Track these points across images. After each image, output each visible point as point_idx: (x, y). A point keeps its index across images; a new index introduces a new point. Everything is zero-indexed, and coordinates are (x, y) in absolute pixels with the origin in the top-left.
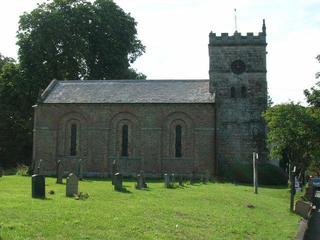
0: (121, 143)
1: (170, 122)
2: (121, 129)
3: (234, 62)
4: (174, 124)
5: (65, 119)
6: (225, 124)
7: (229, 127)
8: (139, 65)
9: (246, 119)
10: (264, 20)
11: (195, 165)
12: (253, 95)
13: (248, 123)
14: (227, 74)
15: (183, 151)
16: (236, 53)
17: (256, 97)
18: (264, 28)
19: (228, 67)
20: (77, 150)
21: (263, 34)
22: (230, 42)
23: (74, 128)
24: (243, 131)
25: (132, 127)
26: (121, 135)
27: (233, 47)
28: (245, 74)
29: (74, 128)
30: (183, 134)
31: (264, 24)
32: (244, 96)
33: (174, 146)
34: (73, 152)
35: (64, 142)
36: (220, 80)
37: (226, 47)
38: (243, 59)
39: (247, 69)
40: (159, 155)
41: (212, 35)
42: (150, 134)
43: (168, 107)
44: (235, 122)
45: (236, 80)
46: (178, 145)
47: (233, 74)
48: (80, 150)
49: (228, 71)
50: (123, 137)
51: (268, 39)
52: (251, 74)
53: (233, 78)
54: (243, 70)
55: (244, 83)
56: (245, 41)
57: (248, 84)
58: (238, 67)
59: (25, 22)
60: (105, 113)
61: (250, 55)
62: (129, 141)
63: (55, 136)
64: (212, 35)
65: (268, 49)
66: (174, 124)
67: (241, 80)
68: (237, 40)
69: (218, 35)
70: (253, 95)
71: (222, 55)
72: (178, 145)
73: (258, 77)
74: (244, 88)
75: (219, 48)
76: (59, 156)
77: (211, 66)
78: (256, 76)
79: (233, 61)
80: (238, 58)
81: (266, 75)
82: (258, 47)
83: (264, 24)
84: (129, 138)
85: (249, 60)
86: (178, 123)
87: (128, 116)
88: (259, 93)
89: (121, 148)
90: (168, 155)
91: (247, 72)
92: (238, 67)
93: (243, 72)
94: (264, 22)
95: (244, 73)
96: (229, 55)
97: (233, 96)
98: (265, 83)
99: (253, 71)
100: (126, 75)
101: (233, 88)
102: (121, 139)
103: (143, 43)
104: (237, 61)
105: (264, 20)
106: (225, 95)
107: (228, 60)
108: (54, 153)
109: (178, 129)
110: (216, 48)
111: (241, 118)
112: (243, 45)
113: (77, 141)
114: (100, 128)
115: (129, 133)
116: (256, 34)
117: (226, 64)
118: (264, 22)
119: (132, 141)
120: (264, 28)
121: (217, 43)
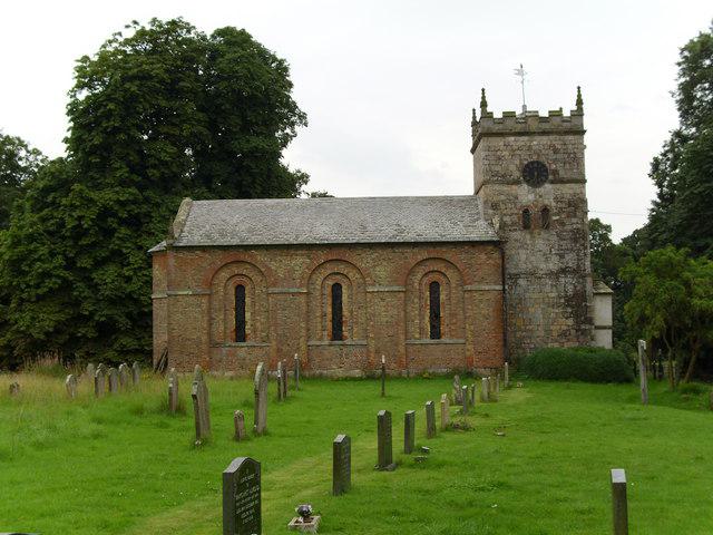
0: (330, 316)
1: (419, 276)
2: (328, 291)
3: (527, 166)
5: (224, 274)
6: (517, 276)
7: (522, 282)
8: (291, 158)
9: (551, 266)
10: (579, 88)
11: (468, 353)
12: (563, 224)
13: (555, 275)
16: (530, 148)
17: (569, 228)
18: (579, 102)
19: (517, 174)
21: (578, 113)
22: (519, 128)
23: (240, 289)
24: (548, 288)
25: (350, 286)
26: (330, 302)
27: (526, 138)
29: (240, 289)
30: (443, 297)
31: (579, 96)
32: (546, 226)
33: (427, 319)
34: (240, 334)
36: (503, 197)
37: (513, 138)
38: (543, 159)
39: (551, 177)
40: (402, 337)
43: (416, 250)
44: (532, 275)
45: (531, 197)
47: (525, 186)
49: (517, 182)
50: (333, 304)
51: (587, 123)
52: (558, 186)
53: (526, 195)
54: (544, 178)
55: (546, 202)
56: (546, 126)
57: (554, 204)
58: (535, 173)
59: (88, 73)
60: (299, 262)
61: (556, 151)
62: (345, 312)
63: (205, 307)
65: (587, 139)
66: (426, 280)
67: (540, 196)
70: (563, 224)
71: (506, 153)
73: (571, 191)
74: (545, 210)
75: (498, 139)
76: (214, 345)
78: (567, 190)
79: (526, 162)
80: (535, 158)
81: (584, 187)
82: (571, 137)
83: (579, 96)
85: (555, 161)
86: (434, 277)
87: (342, 268)
88: (574, 220)
89: (329, 325)
90: (417, 336)
91: (552, 182)
93: (544, 182)
95: (546, 185)
96: (518, 152)
97: (526, 227)
98: (584, 202)
99: (562, 181)
100: (285, 185)
101: (526, 211)
103: (302, 107)
104: (532, 163)
106: (513, 224)
107: (517, 162)
108: (204, 338)
109: (434, 287)
111: (543, 266)
112: (544, 133)
113: (248, 315)
114: (291, 290)
115: (345, 298)
117: (513, 168)
119: (351, 312)
120: (579, 102)
121: (488, 130)
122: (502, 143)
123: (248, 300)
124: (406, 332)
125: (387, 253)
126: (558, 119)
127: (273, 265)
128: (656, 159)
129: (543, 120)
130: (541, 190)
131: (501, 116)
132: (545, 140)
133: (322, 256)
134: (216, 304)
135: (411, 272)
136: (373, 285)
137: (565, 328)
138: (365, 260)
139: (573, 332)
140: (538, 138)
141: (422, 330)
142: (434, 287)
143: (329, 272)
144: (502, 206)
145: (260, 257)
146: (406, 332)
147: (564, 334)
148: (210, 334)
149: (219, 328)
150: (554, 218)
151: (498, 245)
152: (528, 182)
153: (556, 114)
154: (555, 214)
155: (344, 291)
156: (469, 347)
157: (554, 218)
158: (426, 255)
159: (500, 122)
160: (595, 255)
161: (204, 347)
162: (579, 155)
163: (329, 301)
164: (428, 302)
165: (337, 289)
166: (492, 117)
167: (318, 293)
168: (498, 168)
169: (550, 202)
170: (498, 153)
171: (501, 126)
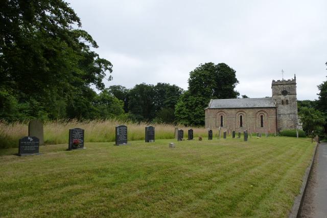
8: (237, 88)
13: (289, 114)
18: (295, 77)
19: (280, 93)
23: (222, 117)
28: (287, 96)
29: (222, 117)
30: (264, 119)
32: (287, 104)
41: (273, 81)
46: (262, 123)
49: (280, 95)
53: (282, 97)
56: (287, 83)
58: (284, 93)
59: (193, 75)
60: (233, 111)
61: (289, 88)
64: (273, 81)
65: (297, 85)
66: (261, 115)
69: (276, 81)
72: (262, 123)
74: (287, 101)
77: (273, 93)
78: (292, 96)
100: (234, 95)
103: (238, 80)
112: (287, 84)
120: (295, 77)
121: (275, 84)
132: (287, 86)
133: (238, 110)
135: (257, 113)
138: (247, 111)
141: (259, 125)
142: (262, 116)
145: (226, 111)
147: (291, 127)
151: (275, 108)
159: (277, 82)
165: (241, 117)
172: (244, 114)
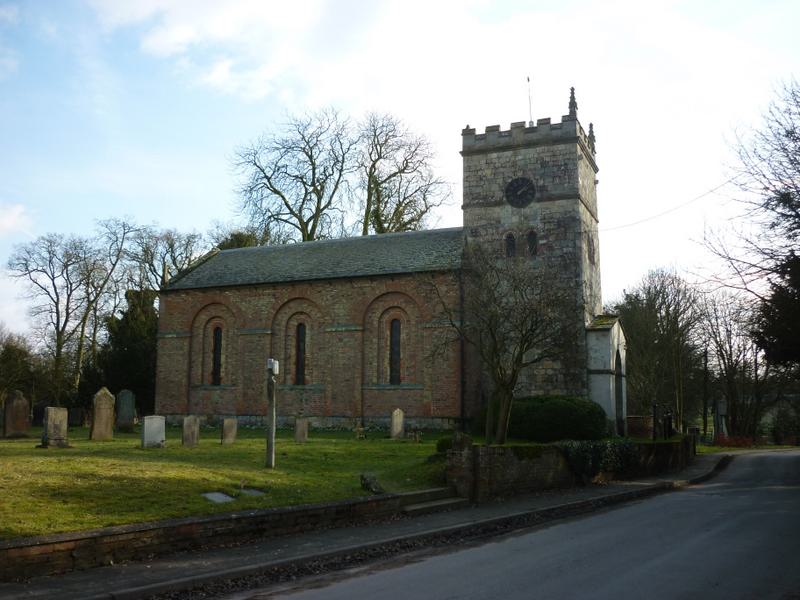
0: (293, 359)
1: (378, 314)
2: (292, 332)
3: (511, 184)
4: (387, 317)
10: (573, 89)
11: (425, 401)
14: (497, 209)
15: (403, 372)
16: (514, 164)
17: (558, 252)
18: (573, 105)
19: (499, 195)
20: (222, 374)
21: (571, 118)
22: (503, 141)
25: (312, 328)
26: (294, 343)
27: (509, 153)
28: (535, 207)
29: (218, 331)
30: (403, 336)
31: (573, 98)
34: (216, 380)
35: (201, 359)
36: (483, 222)
38: (530, 175)
39: (538, 195)
40: (358, 381)
41: (468, 133)
42: (341, 340)
43: (374, 284)
45: (515, 219)
47: (509, 208)
48: (227, 374)
49: (499, 204)
53: (509, 217)
54: (529, 197)
55: (532, 224)
56: (533, 136)
57: (540, 226)
58: (519, 192)
60: (265, 302)
61: (544, 164)
62: (308, 355)
63: (186, 349)
64: (468, 133)
66: (387, 317)
68: (526, 137)
69: (480, 131)
70: (550, 248)
71: (488, 172)
73: (562, 210)
74: (532, 236)
75: (480, 156)
76: (191, 387)
78: (557, 207)
79: (510, 181)
80: (520, 174)
82: (561, 147)
83: (573, 98)
84: (307, 350)
85: (543, 176)
87: (305, 307)
90: (375, 380)
91: (539, 200)
92: (519, 192)
93: (529, 201)
94: (573, 93)
95: (532, 204)
96: (502, 170)
99: (551, 198)
101: (510, 237)
102: (293, 352)
104: (517, 180)
105: (573, 89)
107: (500, 181)
108: (184, 381)
109: (395, 325)
110: (475, 157)
112: (529, 145)
115: (307, 339)
116: (556, 120)
117: (495, 188)
118: (573, 93)
119: (312, 354)
120: (573, 105)
122: (483, 162)
123: (223, 342)
124: (363, 375)
125: (346, 288)
126: (546, 127)
127: (243, 306)
128: (596, 170)
129: (532, 129)
130: (527, 210)
131: (508, 128)
132: (531, 153)
133: (286, 294)
134: (197, 347)
135: (369, 308)
136: (332, 325)
137: (550, 372)
138: (325, 296)
139: (561, 377)
140: (523, 151)
142: (395, 325)
143: (294, 311)
144: (483, 233)
145: (232, 297)
146: (363, 375)
147: (548, 380)
148: (189, 377)
149: (197, 371)
150: (541, 242)
152: (512, 203)
153: (545, 122)
154: (542, 238)
155: (307, 332)
156: (427, 393)
157: (541, 242)
158: (384, 289)
159: (482, 137)
160: (126, 295)
161: (184, 390)
162: (570, 167)
163: (293, 343)
164: (389, 343)
165: (301, 328)
166: (549, 123)
167: (283, 334)
168: (479, 190)
169: (538, 225)
170: (480, 173)
171: (507, 139)
172: (315, 314)
